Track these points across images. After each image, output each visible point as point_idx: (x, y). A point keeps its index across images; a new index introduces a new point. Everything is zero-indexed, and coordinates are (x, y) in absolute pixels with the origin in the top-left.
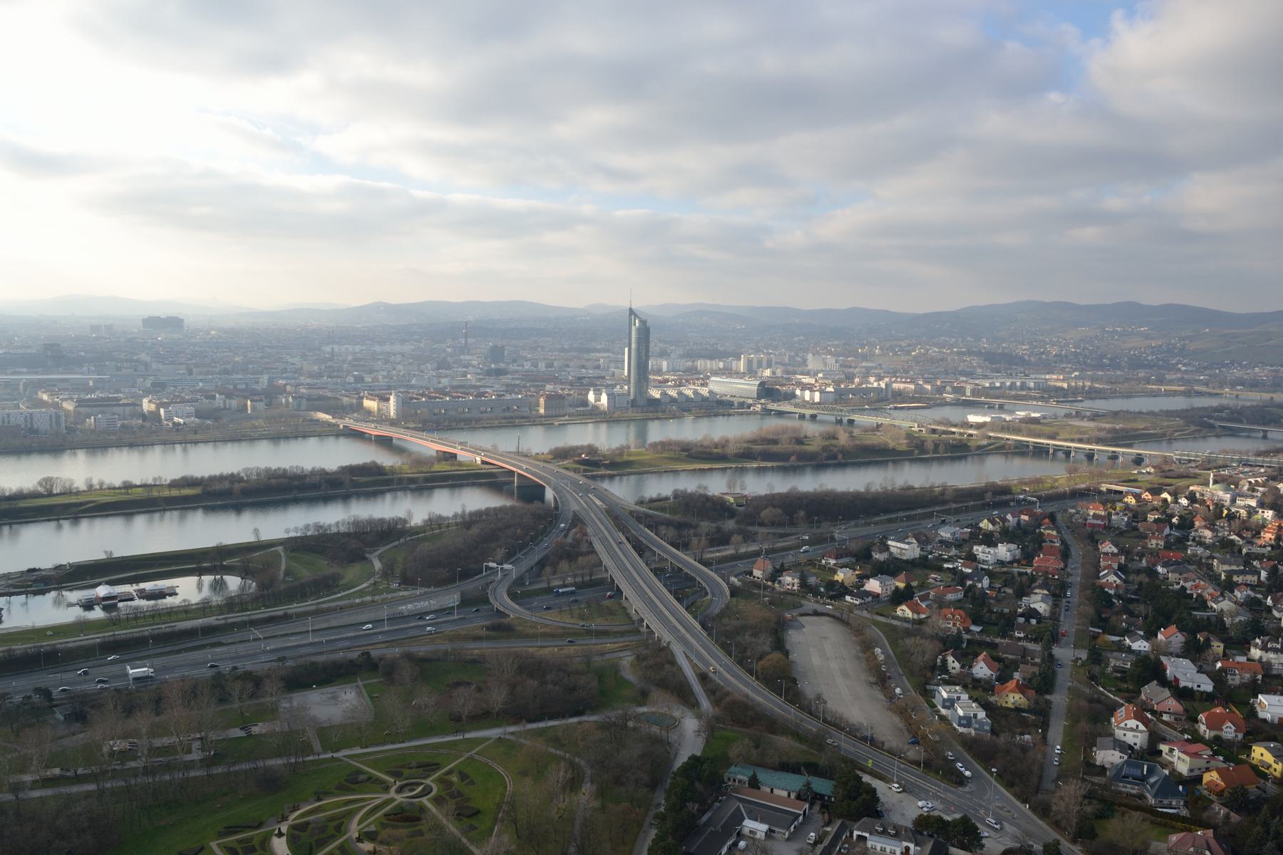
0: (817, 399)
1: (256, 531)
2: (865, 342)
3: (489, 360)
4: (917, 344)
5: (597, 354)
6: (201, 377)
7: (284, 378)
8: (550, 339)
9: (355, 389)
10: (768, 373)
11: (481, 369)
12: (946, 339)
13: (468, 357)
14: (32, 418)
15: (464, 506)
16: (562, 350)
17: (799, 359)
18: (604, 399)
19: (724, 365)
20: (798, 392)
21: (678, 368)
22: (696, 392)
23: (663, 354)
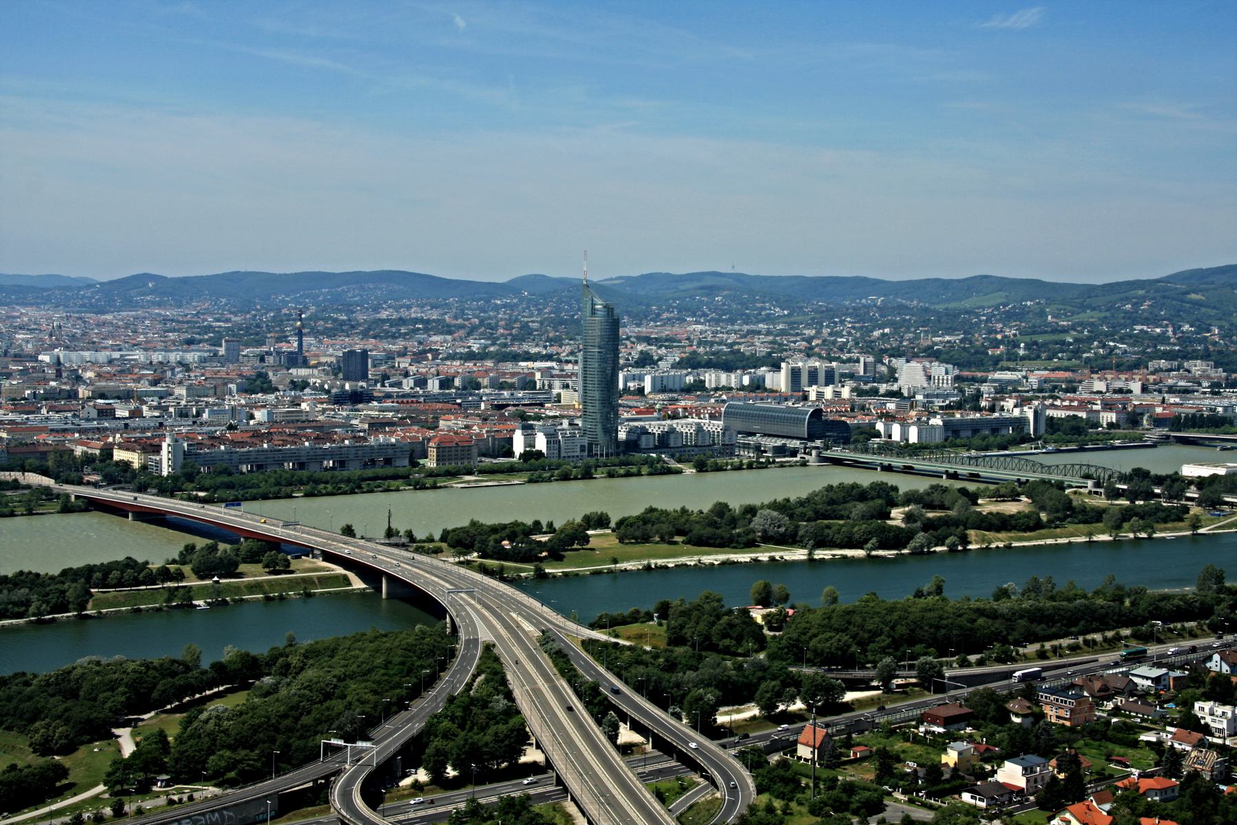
0: (913, 437)
2: (999, 337)
3: (341, 376)
4: (1090, 340)
5: (530, 364)
8: (449, 337)
10: (828, 392)
11: (328, 392)
12: (1145, 328)
13: (303, 372)
16: (471, 356)
17: (884, 369)
18: (541, 443)
19: (751, 380)
20: (880, 426)
21: (671, 386)
22: (699, 429)
23: (645, 361)
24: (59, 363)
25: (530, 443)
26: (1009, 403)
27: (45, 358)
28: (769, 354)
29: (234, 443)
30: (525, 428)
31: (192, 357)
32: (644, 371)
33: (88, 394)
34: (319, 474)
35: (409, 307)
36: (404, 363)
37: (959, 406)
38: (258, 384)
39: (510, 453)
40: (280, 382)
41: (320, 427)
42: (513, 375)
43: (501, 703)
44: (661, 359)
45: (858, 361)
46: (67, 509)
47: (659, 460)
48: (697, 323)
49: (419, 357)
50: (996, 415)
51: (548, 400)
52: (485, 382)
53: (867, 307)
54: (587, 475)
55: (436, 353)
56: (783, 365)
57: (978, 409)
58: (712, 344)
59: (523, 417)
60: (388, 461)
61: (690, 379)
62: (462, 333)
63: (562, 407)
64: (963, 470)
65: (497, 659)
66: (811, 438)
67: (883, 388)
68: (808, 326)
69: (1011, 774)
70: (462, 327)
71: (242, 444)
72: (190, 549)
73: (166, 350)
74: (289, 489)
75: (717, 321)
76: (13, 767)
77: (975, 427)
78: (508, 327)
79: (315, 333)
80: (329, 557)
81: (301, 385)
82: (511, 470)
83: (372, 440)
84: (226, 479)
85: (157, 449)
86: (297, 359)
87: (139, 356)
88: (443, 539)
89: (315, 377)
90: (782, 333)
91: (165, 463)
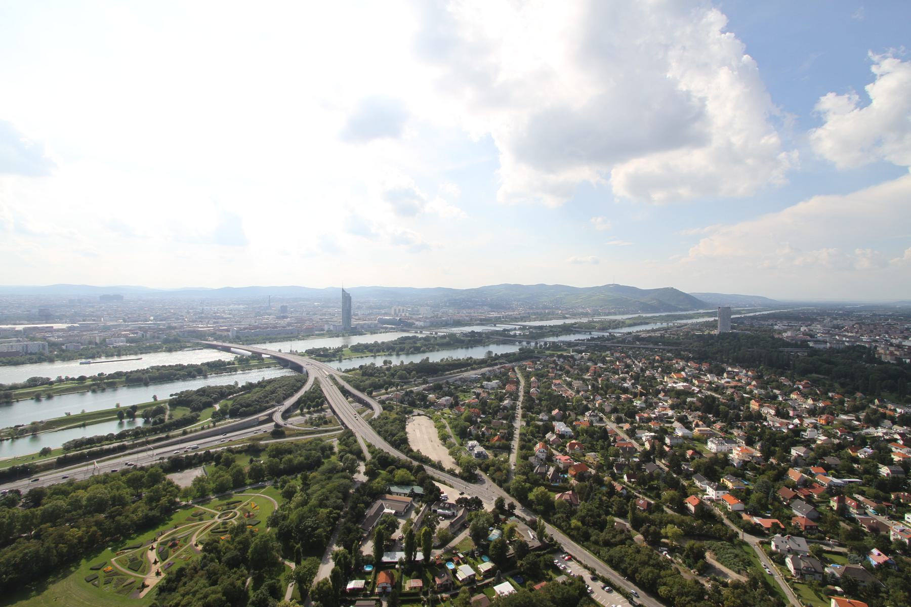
1: (155, 397)
15: (264, 378)
60: (292, 333)
65: (318, 382)
72: (236, 357)
76: (184, 415)
83: (288, 328)
88: (306, 352)
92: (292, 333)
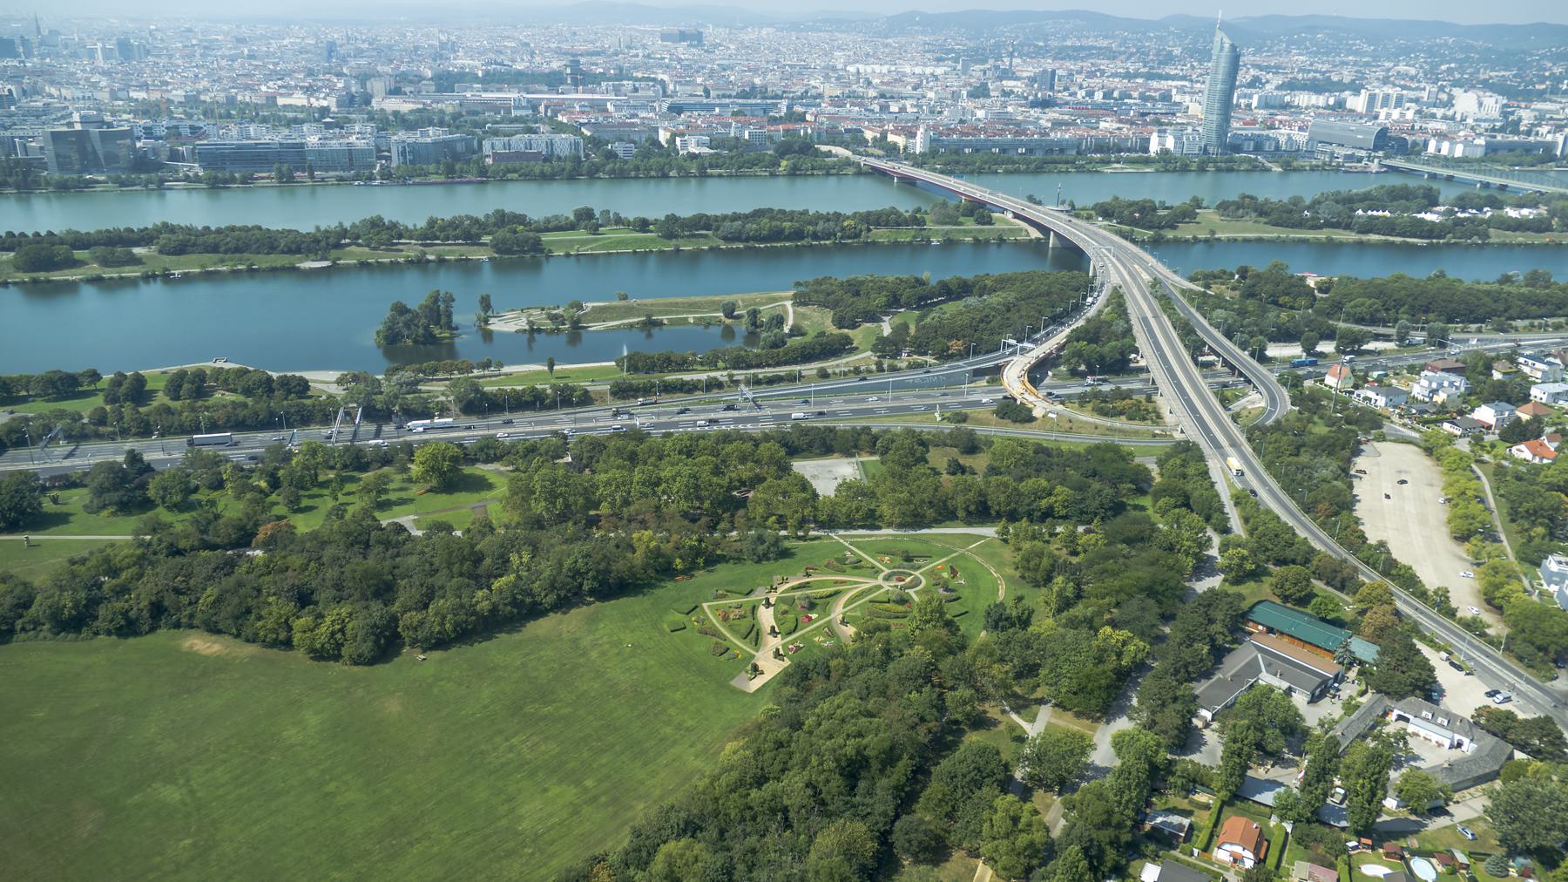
5: (1170, 83)
6: (718, 101)
7: (802, 105)
9: (881, 120)
10: (1396, 114)
11: (1026, 98)
13: (1011, 83)
14: (552, 145)
22: (1290, 138)
23: (1255, 83)
24: (858, 73)
25: (1162, 144)
26: (1544, 130)
27: (851, 69)
28: (1353, 81)
29: (962, 134)
30: (1159, 131)
31: (939, 71)
32: (1254, 91)
33: (875, 94)
34: (1016, 158)
35: (1088, 38)
36: (1079, 79)
37: (1502, 130)
38: (980, 92)
39: (1146, 150)
40: (997, 88)
41: (1018, 124)
42: (1156, 90)
43: (1120, 326)
44: (1268, 82)
45: (1424, 89)
46: (860, 173)
47: (1256, 160)
48: (1299, 54)
49: (1091, 75)
50: (1532, 139)
51: (1179, 111)
52: (1135, 94)
53: (1440, 46)
54: (1202, 169)
55: (1103, 72)
56: (1363, 91)
57: (1517, 133)
58: (1309, 71)
59: (1158, 123)
61: (1287, 99)
62: (1123, 57)
63: (1188, 117)
64: (1495, 181)
66: (1376, 148)
67: (1440, 112)
68: (1388, 59)
69: (1485, 414)
70: (1124, 53)
71: (967, 134)
73: (925, 65)
74: (994, 167)
75: (1316, 54)
77: (1511, 148)
78: (1158, 54)
79: (1020, 56)
80: (1017, 216)
81: (1006, 94)
82: (1148, 162)
84: (956, 157)
85: (913, 135)
86: (1008, 74)
87: (908, 69)
89: (1017, 86)
90: (1367, 64)
91: (919, 145)
92: (1062, 151)
